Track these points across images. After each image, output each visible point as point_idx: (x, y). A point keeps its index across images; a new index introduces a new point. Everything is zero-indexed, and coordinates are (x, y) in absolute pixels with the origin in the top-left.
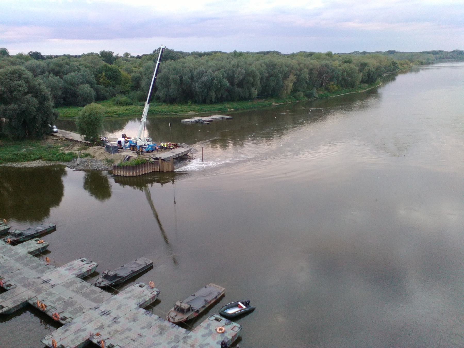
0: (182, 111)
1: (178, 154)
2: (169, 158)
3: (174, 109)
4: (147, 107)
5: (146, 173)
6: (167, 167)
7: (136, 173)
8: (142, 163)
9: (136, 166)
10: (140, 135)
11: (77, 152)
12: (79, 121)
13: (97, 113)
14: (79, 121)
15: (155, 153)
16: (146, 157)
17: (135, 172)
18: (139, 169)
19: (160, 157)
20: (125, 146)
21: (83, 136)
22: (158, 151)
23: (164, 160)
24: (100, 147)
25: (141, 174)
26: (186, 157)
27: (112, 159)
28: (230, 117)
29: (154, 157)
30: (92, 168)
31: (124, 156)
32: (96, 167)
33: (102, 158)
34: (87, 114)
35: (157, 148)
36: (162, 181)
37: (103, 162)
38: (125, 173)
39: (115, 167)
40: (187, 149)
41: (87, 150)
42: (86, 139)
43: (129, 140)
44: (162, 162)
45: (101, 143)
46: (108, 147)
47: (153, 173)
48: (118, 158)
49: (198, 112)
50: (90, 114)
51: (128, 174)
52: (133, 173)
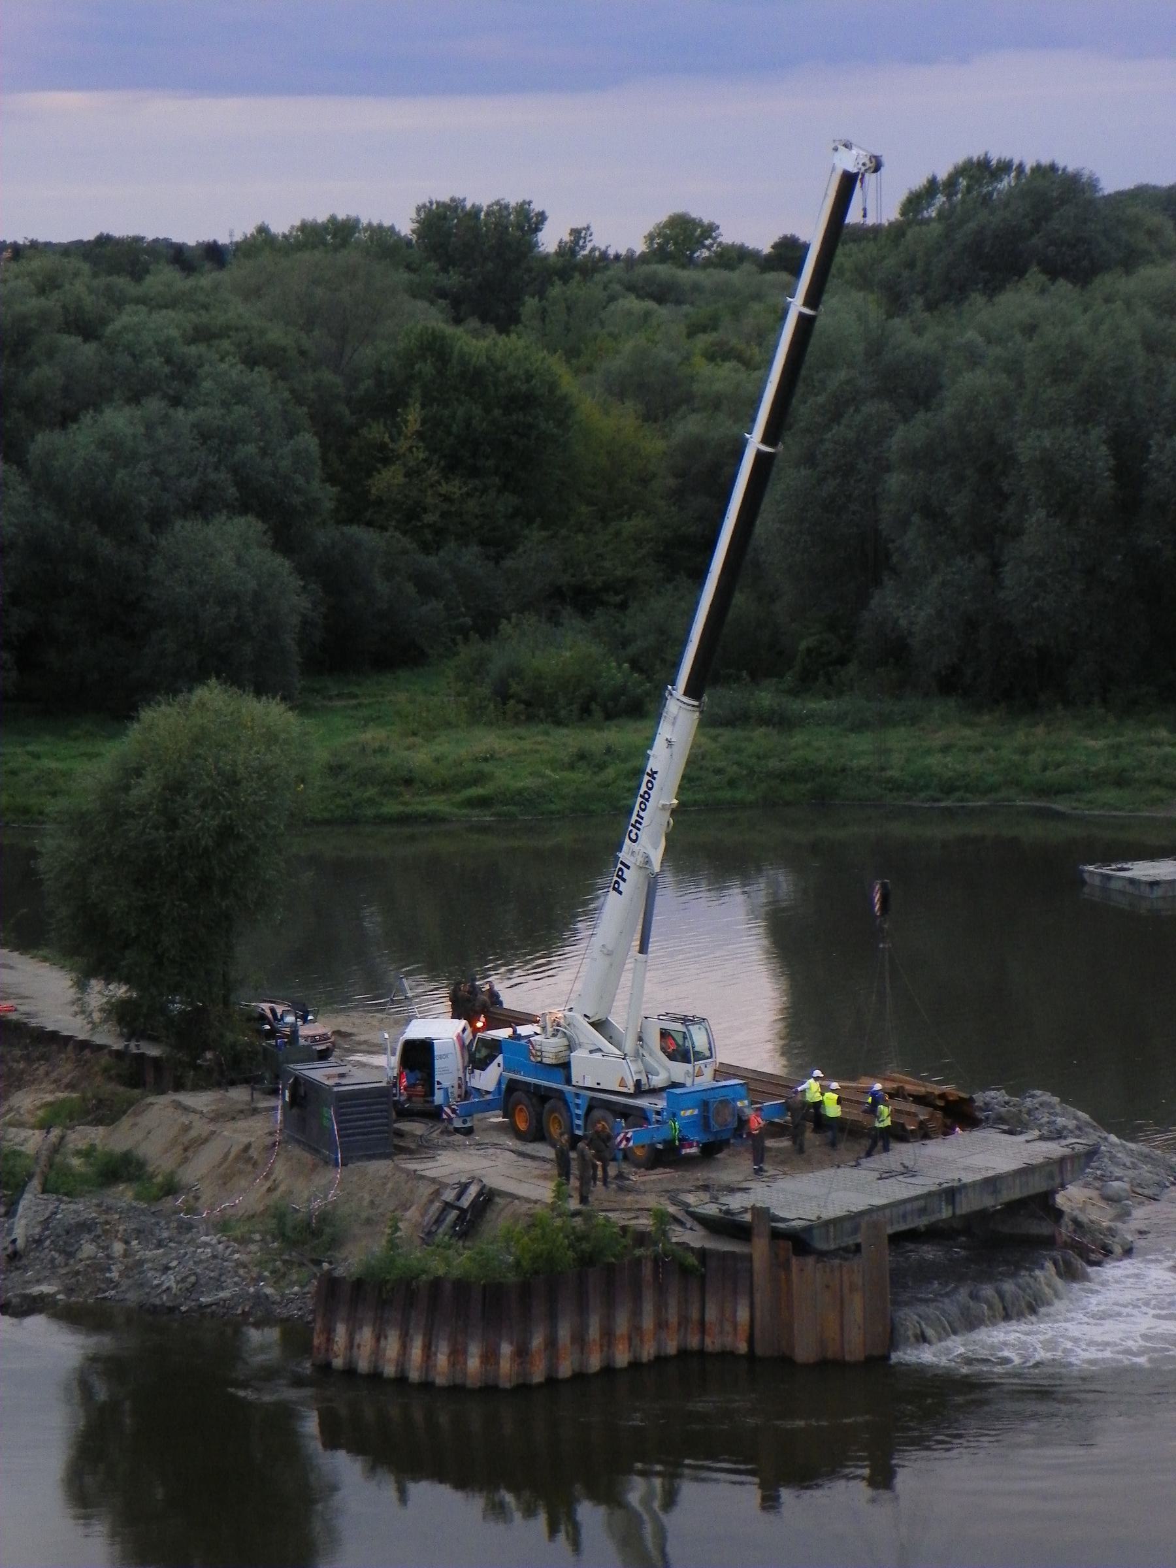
0: (1121, 780)
1: (951, 1194)
2: (854, 1219)
3: (1035, 759)
4: (673, 736)
5: (622, 1358)
6: (827, 1317)
7: (522, 1352)
8: (587, 1261)
9: (526, 1290)
10: (607, 991)
11: (31, 1141)
12: (74, 845)
13: (233, 782)
14: (74, 845)
15: (733, 1168)
16: (642, 1202)
17: (506, 1349)
18: (552, 1318)
19: (762, 1213)
20: (467, 1092)
21: (100, 993)
22: (760, 1156)
23: (797, 1241)
24: (239, 1095)
25: (565, 1369)
26: (1044, 1229)
27: (325, 1218)
29: (712, 1210)
30: (133, 1297)
31: (439, 1186)
32: (170, 1280)
33: (248, 1197)
34: (146, 788)
35: (757, 1123)
36: (786, 1468)
37: (244, 1241)
38: (416, 1352)
39: (331, 1288)
40: (1055, 1149)
41: (125, 1122)
42: (123, 1015)
43: (503, 1033)
44: (780, 1265)
45: (258, 1062)
46: (304, 1097)
47: (694, 1367)
48: (388, 1203)
50: (176, 787)
51: (442, 1360)
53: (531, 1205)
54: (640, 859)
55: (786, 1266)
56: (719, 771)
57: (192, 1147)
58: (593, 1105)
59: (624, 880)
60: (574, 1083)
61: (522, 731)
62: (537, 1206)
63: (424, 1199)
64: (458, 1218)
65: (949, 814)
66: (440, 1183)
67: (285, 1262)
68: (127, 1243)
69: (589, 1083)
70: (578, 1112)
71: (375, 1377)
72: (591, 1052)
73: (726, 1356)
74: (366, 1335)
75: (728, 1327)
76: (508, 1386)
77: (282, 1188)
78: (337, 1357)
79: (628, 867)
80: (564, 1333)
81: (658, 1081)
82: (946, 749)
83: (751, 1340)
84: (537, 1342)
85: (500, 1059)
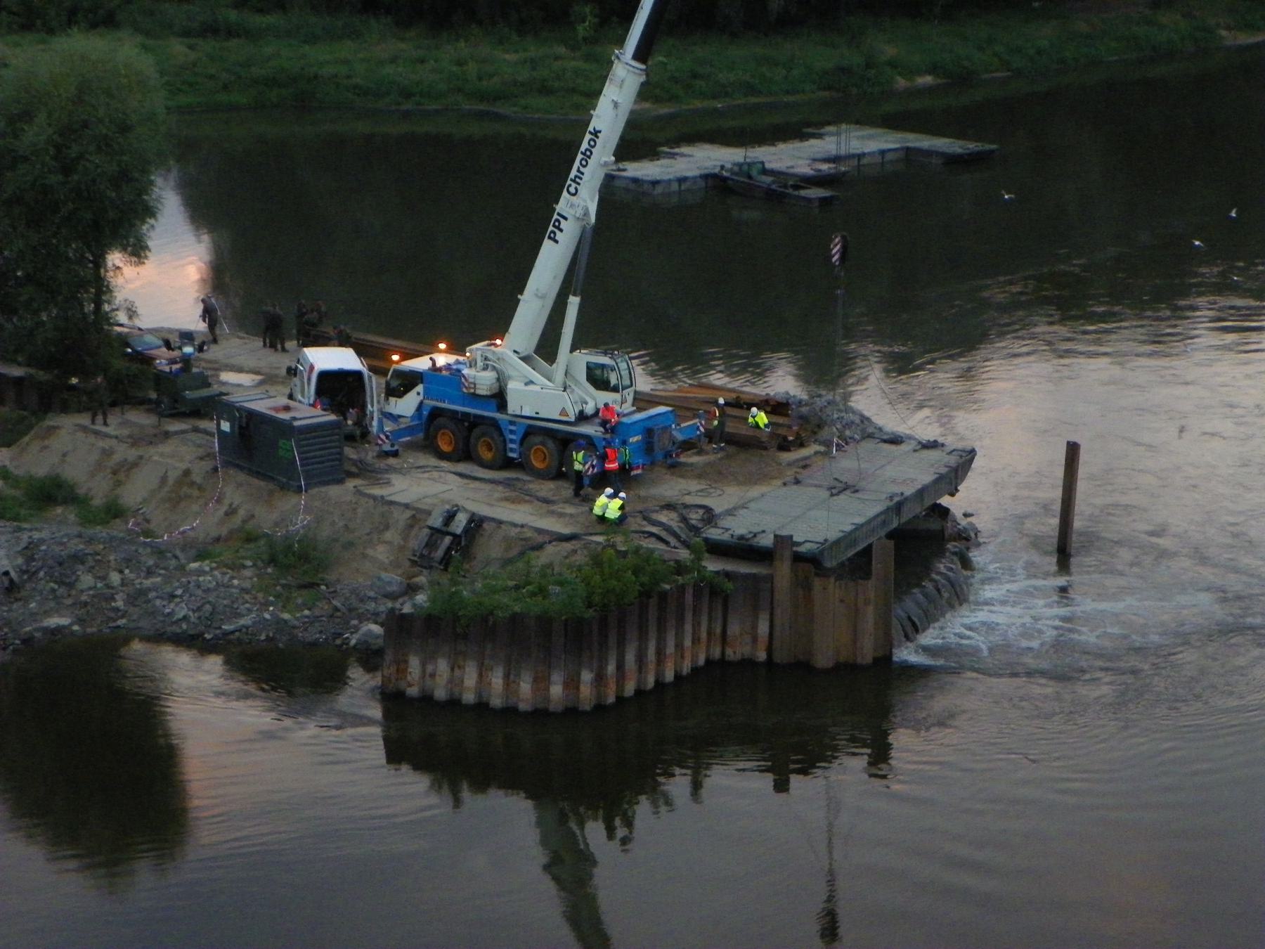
0: (545, 90)
3: (472, 68)
7: (600, 678)
8: (646, 594)
13: (125, 129)
17: (587, 676)
23: (809, 563)
28: (972, 146)
31: (417, 515)
44: (802, 585)
47: (717, 675)
49: (673, 98)
51: (525, 687)
52: (572, 683)
53: (518, 530)
54: (579, 212)
55: (808, 588)
56: (212, 77)
57: (124, 470)
58: (530, 432)
59: (561, 230)
60: (510, 411)
61: (16, 38)
62: (525, 530)
63: (402, 524)
64: (452, 543)
65: (406, 115)
66: (415, 509)
67: (283, 586)
68: (121, 572)
69: (526, 412)
70: (513, 437)
71: (453, 704)
72: (526, 384)
73: (748, 664)
74: (442, 666)
75: (748, 639)
76: (588, 708)
77: (242, 513)
78: (410, 685)
79: (565, 219)
80: (630, 657)
81: (589, 409)
82: (394, 60)
83: (770, 650)
84: (611, 668)
85: (420, 388)
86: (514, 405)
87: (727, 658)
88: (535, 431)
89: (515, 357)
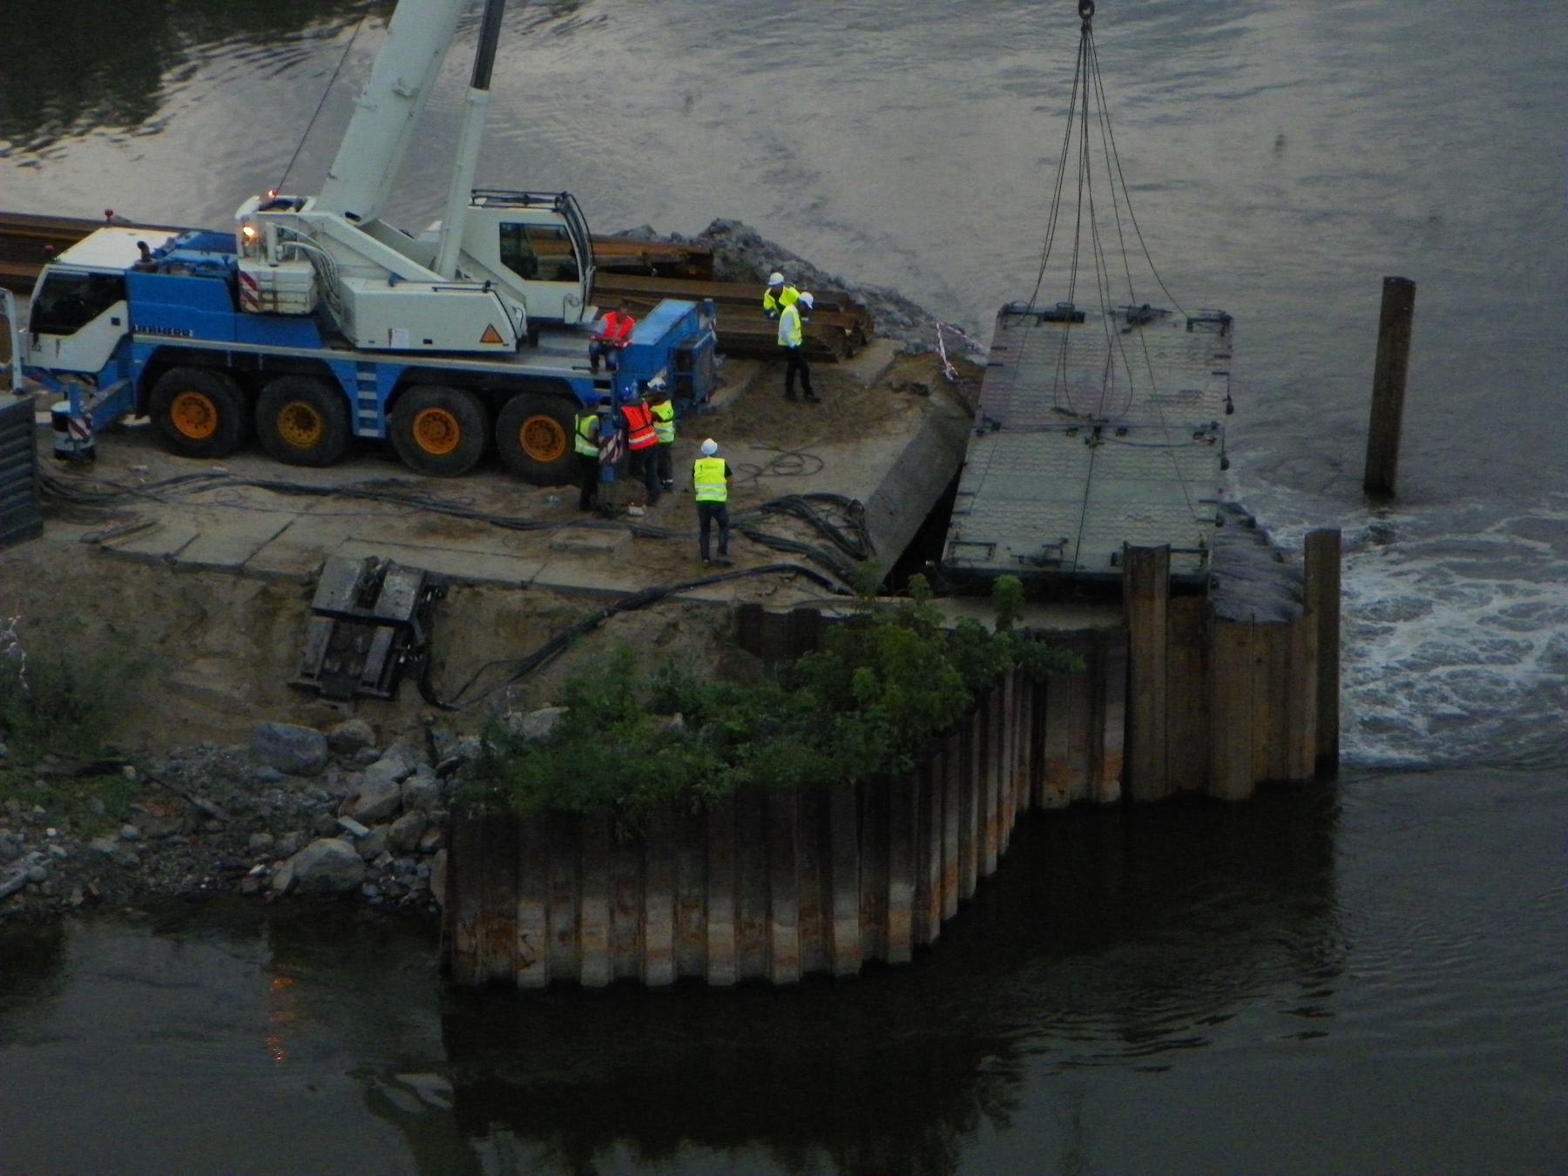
51: (786, 934)
52: (876, 912)
58: (409, 381)
64: (394, 639)
67: (46, 777)
83: (1126, 778)
85: (119, 309)
86: (367, 332)
87: (1045, 804)
88: (419, 380)
89: (349, 225)
